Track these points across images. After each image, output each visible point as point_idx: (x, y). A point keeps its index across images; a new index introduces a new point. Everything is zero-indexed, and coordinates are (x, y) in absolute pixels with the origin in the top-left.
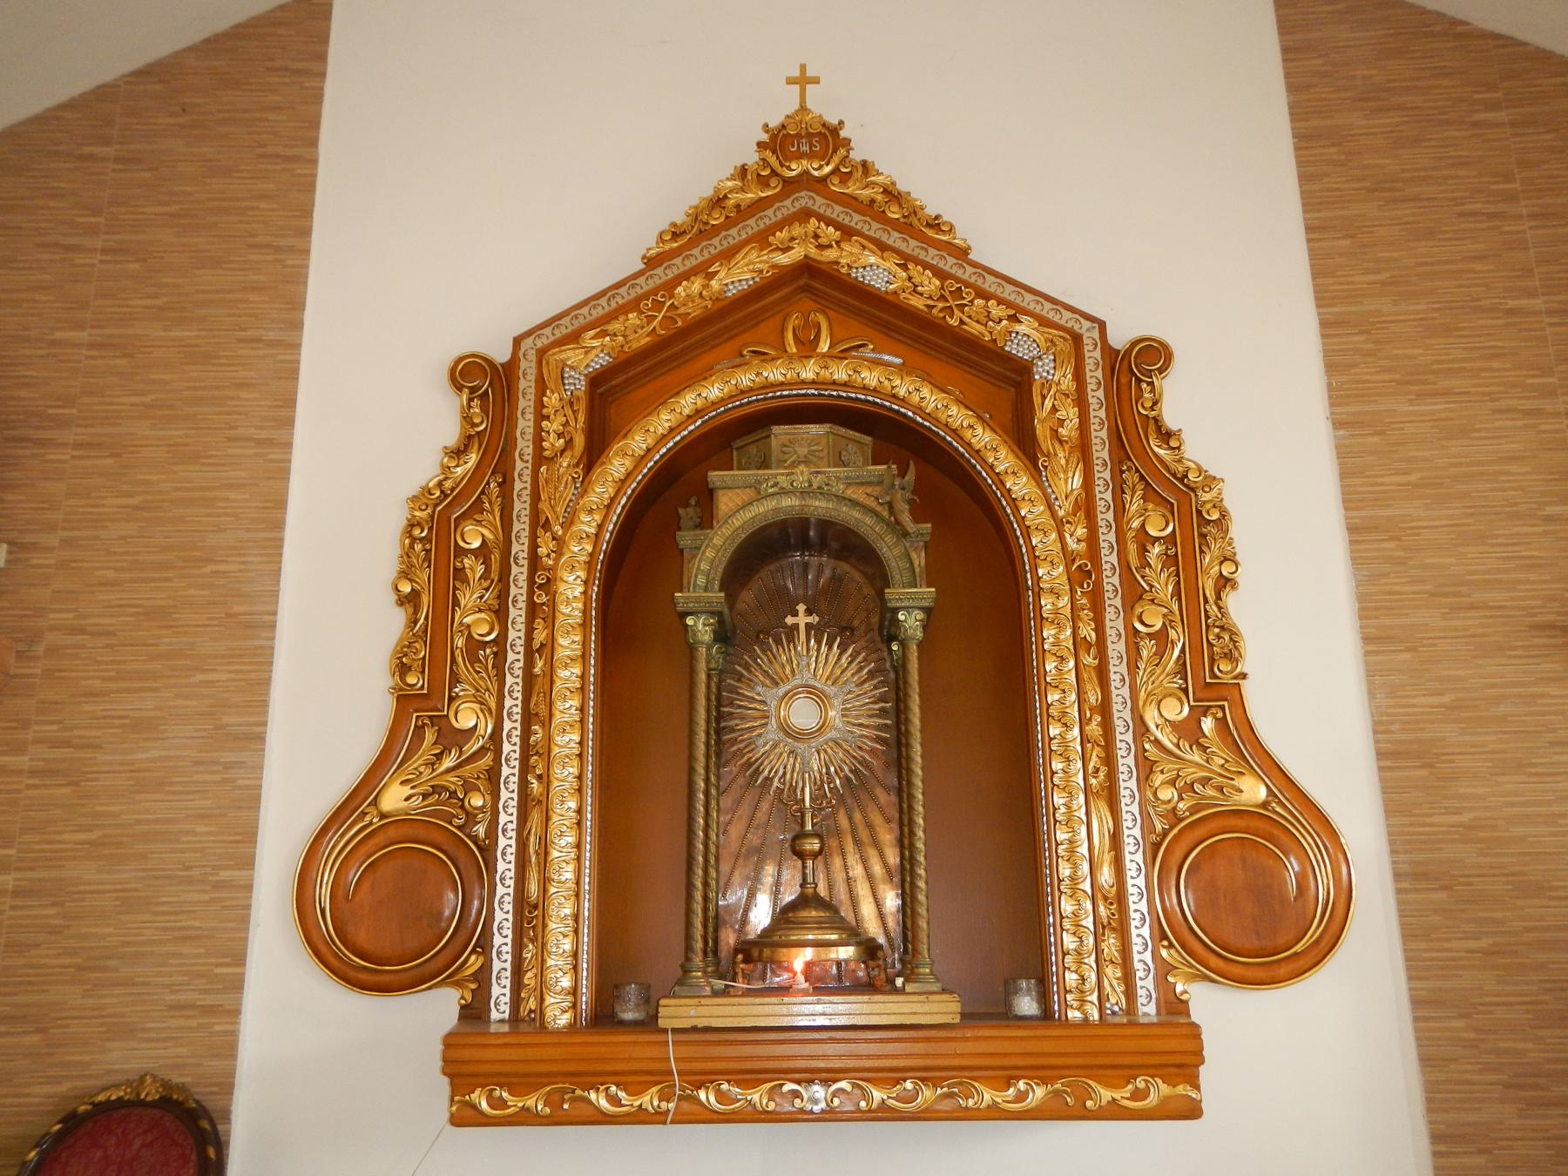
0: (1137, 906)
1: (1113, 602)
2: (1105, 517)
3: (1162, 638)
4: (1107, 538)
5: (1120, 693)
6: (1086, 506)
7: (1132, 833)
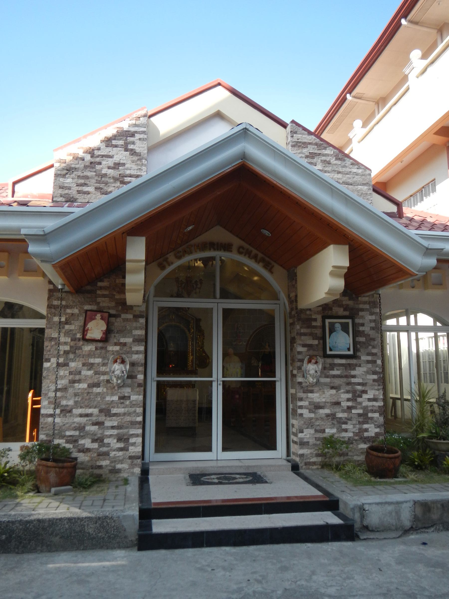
0: (194, 363)
1: (194, 341)
2: (195, 334)
3: (198, 343)
4: (195, 335)
5: (194, 347)
6: (193, 332)
7: (194, 357)
